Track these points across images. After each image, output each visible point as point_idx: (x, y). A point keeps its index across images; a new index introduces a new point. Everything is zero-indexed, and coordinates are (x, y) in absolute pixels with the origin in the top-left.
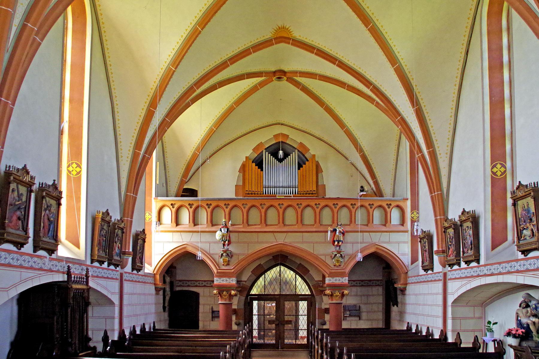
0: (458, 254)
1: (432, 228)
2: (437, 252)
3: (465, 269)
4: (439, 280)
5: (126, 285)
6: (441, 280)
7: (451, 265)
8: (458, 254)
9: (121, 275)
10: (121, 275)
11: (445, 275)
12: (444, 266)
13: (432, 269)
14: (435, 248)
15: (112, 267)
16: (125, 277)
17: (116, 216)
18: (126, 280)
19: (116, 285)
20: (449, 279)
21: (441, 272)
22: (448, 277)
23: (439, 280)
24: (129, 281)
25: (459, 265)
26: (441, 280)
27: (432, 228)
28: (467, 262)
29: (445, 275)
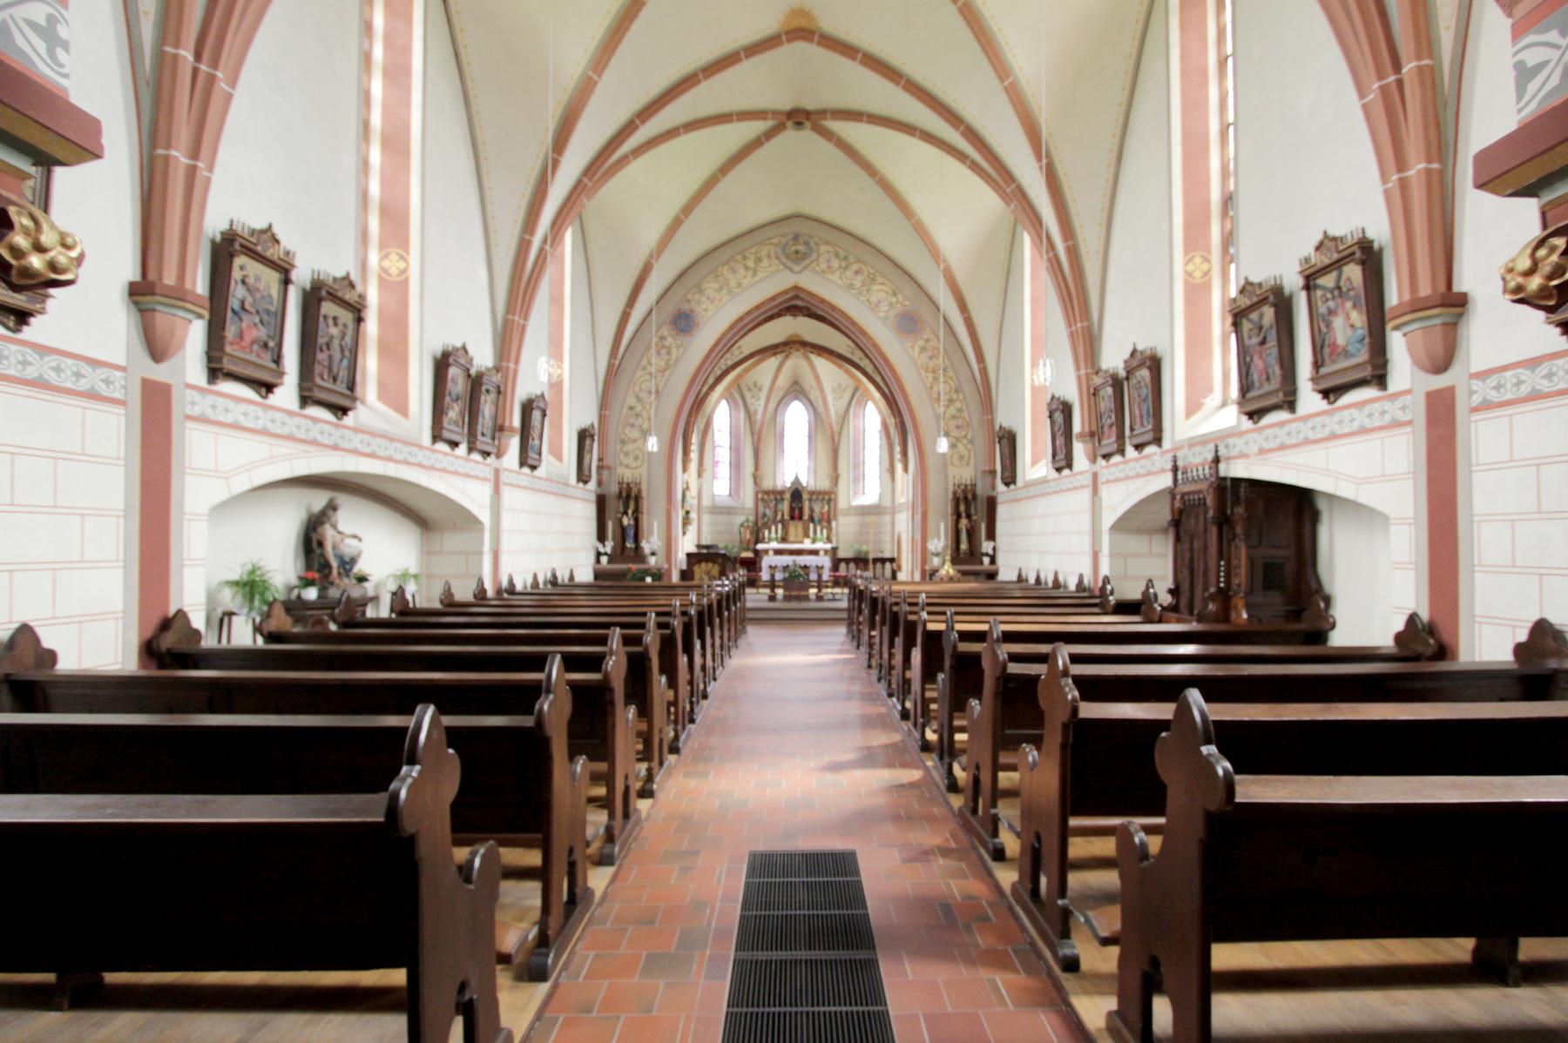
0: (1121, 437)
1: (1070, 391)
2: (1081, 435)
3: (1136, 460)
4: (1083, 487)
5: (506, 492)
6: (1087, 486)
7: (1106, 457)
8: (1121, 437)
9: (497, 472)
10: (497, 472)
11: (1095, 476)
12: (1093, 460)
13: (1070, 466)
14: (1077, 427)
15: (476, 456)
16: (504, 477)
17: (483, 357)
18: (505, 484)
19: (486, 490)
20: (1103, 483)
21: (1086, 472)
22: (1101, 479)
23: (1083, 487)
24: (511, 485)
25: (1121, 451)
26: (1087, 486)
27: (1070, 391)
28: (1139, 447)
29: (1095, 476)
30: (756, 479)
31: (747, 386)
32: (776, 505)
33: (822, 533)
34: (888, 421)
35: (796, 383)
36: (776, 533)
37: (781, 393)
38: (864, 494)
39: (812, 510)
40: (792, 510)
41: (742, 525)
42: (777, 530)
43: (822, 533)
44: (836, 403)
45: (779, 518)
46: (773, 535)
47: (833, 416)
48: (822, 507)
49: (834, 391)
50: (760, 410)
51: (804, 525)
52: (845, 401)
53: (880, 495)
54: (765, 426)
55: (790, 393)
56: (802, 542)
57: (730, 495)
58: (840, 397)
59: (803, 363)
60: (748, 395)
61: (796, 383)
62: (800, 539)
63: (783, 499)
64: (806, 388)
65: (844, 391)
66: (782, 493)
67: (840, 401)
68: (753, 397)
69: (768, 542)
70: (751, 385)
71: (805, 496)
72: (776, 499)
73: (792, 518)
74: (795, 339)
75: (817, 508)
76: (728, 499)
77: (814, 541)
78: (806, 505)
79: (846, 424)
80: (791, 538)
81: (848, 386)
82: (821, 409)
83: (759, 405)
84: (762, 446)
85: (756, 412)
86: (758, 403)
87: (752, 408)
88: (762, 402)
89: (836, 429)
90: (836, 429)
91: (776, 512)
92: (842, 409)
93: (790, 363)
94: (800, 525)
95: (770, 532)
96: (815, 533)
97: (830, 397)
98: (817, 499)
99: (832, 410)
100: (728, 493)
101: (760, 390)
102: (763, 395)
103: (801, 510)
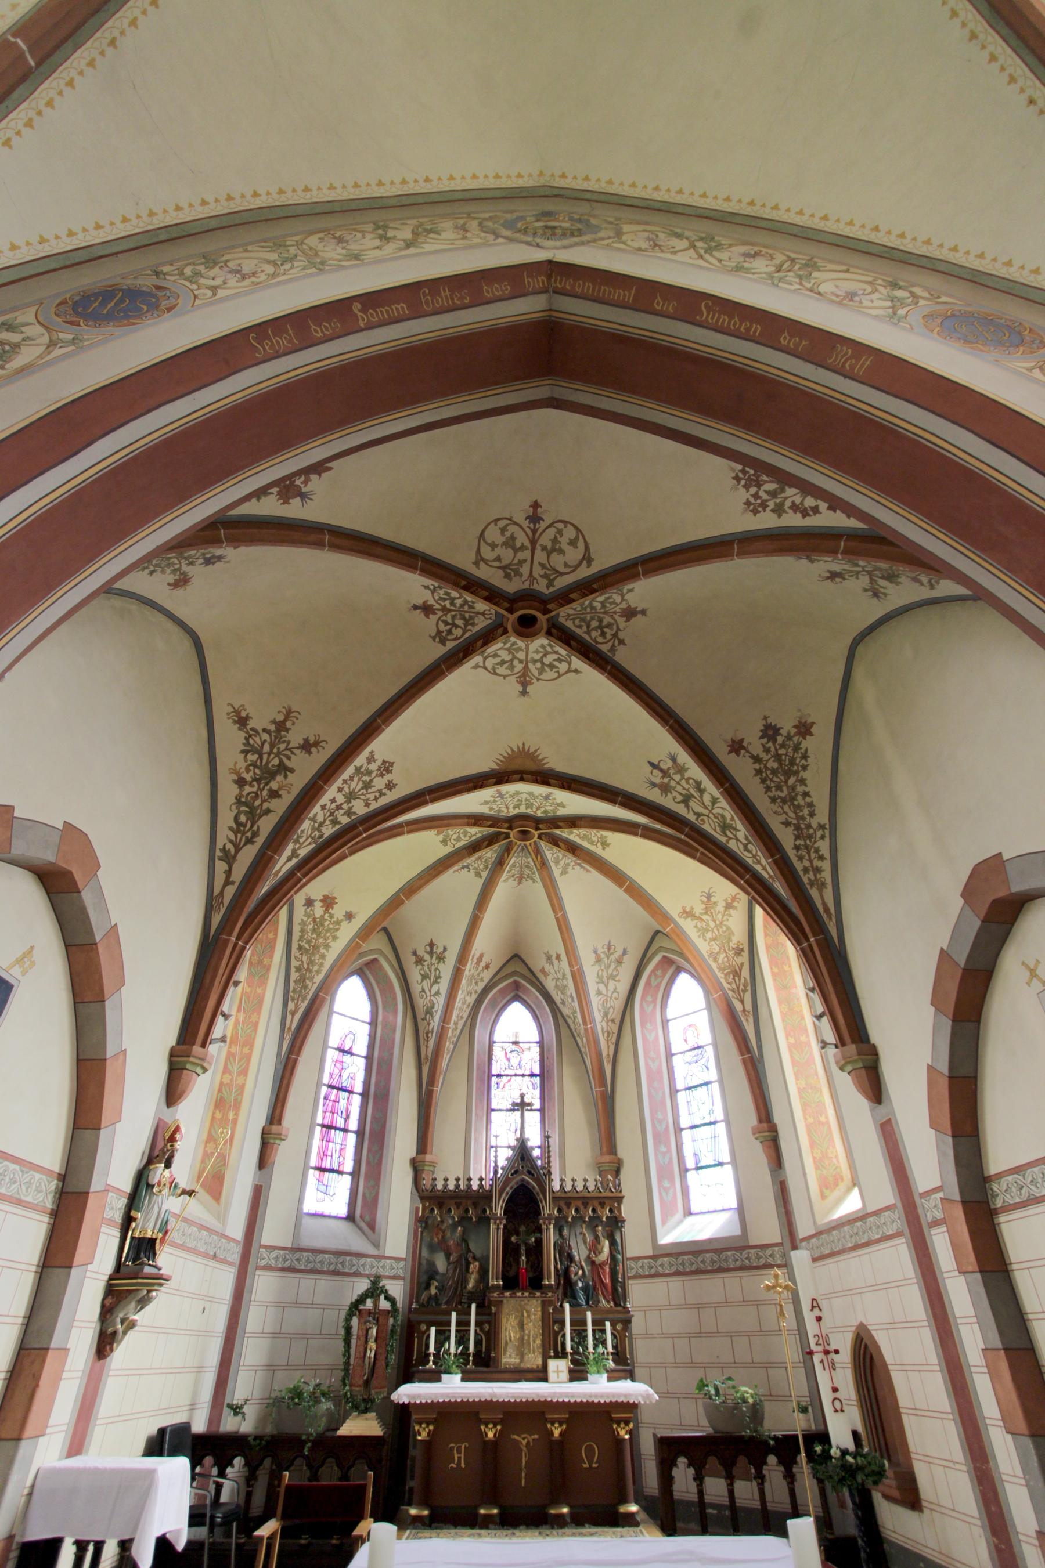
30: (417, 1167)
31: (415, 953)
32: (464, 1240)
33: (600, 1341)
34: (738, 1007)
35: (516, 957)
36: (462, 1340)
37: (487, 976)
38: (688, 1213)
39: (566, 1255)
40: (510, 1251)
41: (355, 1307)
42: (463, 1324)
43: (600, 1341)
44: (602, 987)
45: (471, 1285)
46: (452, 1346)
47: (598, 1017)
48: (595, 1247)
49: (598, 960)
50: (440, 1002)
51: (545, 1305)
52: (623, 986)
53: (741, 1210)
54: (449, 1045)
55: (506, 977)
56: (541, 1375)
57: (350, 1217)
58: (612, 977)
59: (536, 889)
60: (415, 974)
61: (516, 957)
62: (534, 1360)
63: (484, 1220)
64: (538, 963)
65: (619, 962)
66: (481, 1199)
67: (612, 984)
68: (425, 977)
69: (434, 1377)
70: (421, 952)
71: (548, 1210)
72: (464, 1219)
73: (511, 1283)
74: (517, 765)
75: (580, 1252)
76: (345, 1227)
77: (578, 1374)
78: (551, 1236)
79: (626, 1040)
80: (509, 1358)
81: (625, 952)
82: (570, 1007)
83: (438, 993)
84: (437, 1089)
85: (429, 1011)
86: (435, 988)
87: (421, 1003)
88: (444, 985)
89: (606, 1049)
90: (606, 1049)
91: (462, 1264)
92: (619, 1004)
93: (504, 889)
94: (533, 1308)
95: (443, 1337)
96: (580, 1335)
97: (591, 973)
98: (579, 1219)
99: (596, 1002)
100: (343, 1211)
101: (441, 958)
102: (446, 971)
103: (536, 1251)
